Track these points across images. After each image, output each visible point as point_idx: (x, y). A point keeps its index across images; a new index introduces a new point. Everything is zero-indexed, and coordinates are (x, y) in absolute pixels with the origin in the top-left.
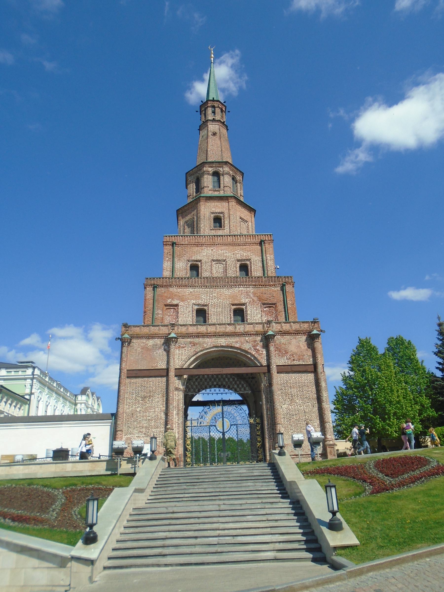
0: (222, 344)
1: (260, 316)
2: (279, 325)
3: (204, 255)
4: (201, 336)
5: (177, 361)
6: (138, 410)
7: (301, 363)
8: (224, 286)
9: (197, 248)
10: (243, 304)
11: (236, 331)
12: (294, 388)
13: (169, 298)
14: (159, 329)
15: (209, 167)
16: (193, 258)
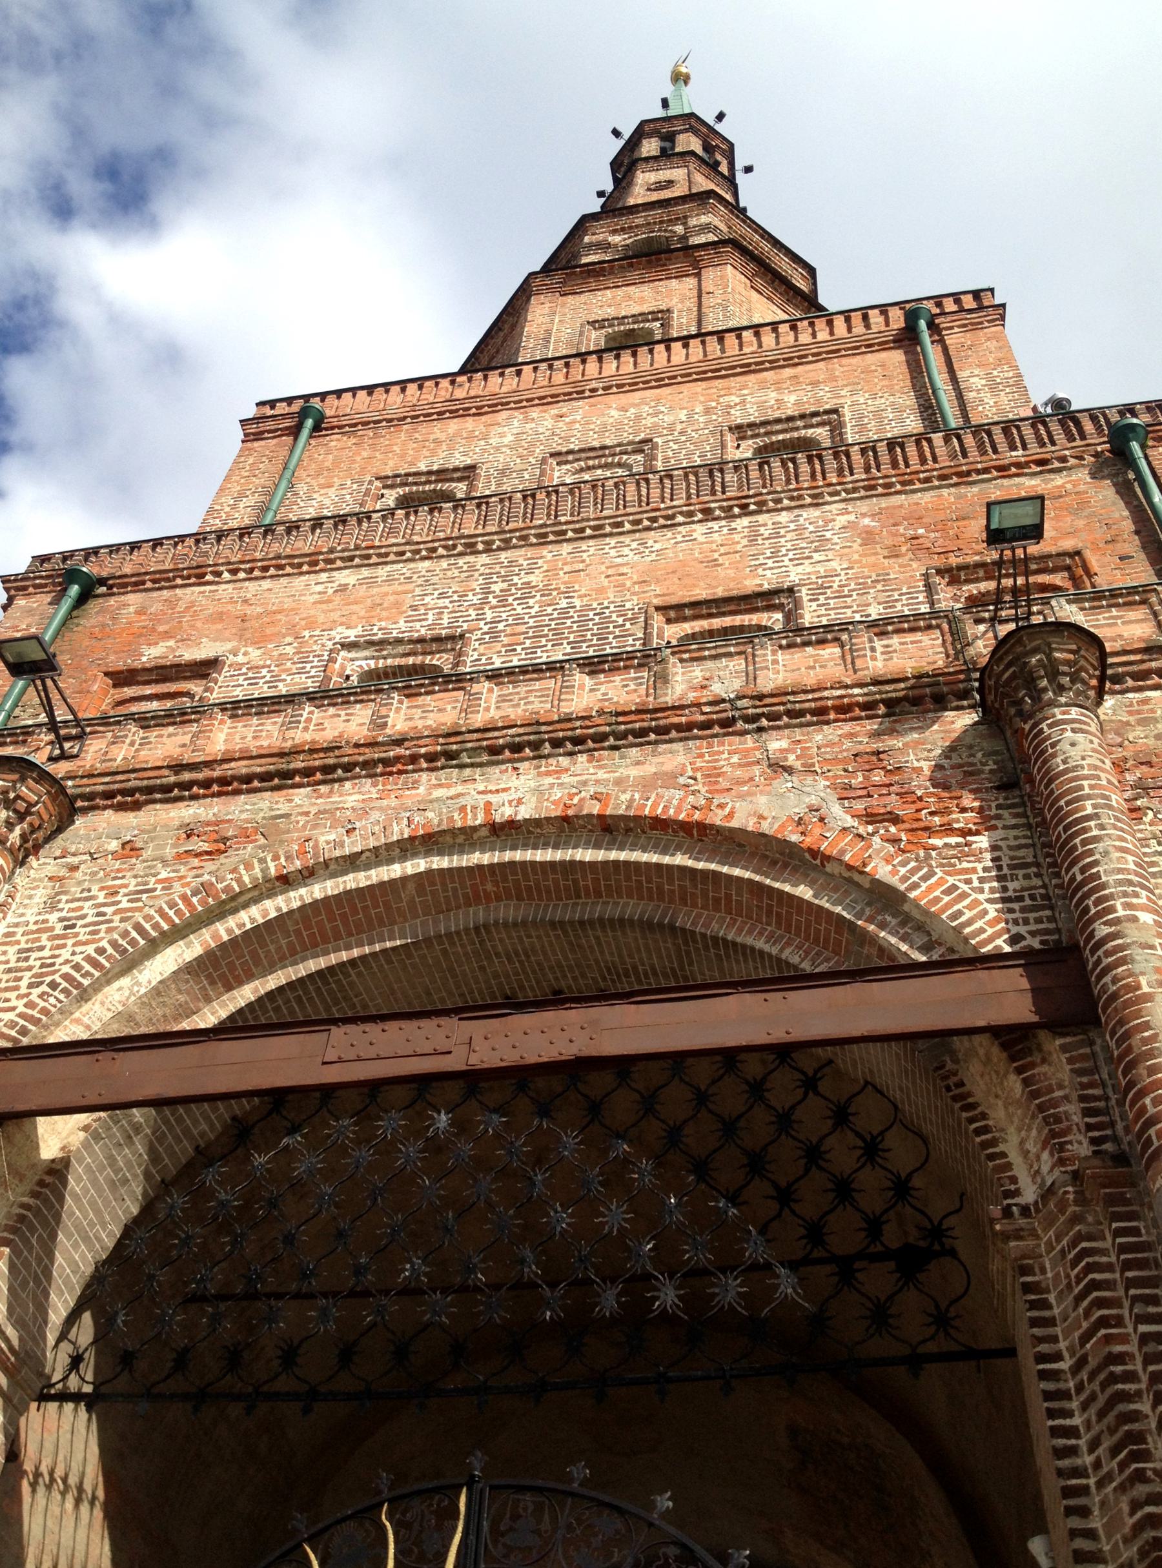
0: (504, 813)
2: (1133, 615)
4: (308, 772)
9: (453, 425)
11: (669, 699)
13: (167, 635)
15: (615, 232)
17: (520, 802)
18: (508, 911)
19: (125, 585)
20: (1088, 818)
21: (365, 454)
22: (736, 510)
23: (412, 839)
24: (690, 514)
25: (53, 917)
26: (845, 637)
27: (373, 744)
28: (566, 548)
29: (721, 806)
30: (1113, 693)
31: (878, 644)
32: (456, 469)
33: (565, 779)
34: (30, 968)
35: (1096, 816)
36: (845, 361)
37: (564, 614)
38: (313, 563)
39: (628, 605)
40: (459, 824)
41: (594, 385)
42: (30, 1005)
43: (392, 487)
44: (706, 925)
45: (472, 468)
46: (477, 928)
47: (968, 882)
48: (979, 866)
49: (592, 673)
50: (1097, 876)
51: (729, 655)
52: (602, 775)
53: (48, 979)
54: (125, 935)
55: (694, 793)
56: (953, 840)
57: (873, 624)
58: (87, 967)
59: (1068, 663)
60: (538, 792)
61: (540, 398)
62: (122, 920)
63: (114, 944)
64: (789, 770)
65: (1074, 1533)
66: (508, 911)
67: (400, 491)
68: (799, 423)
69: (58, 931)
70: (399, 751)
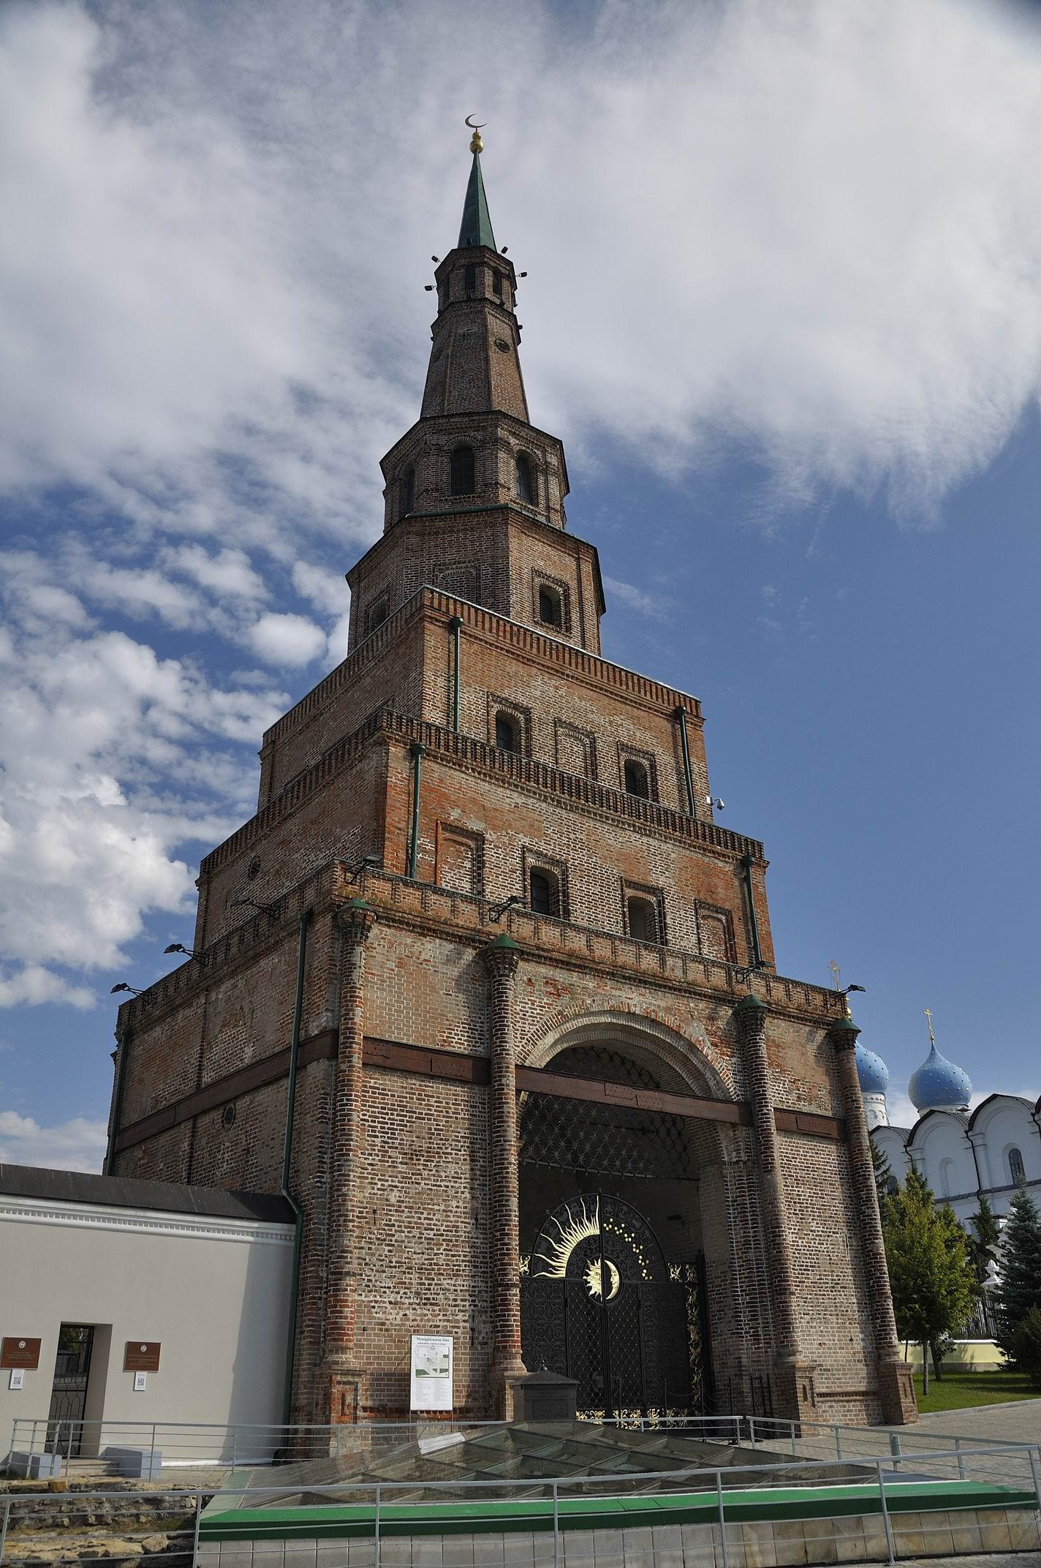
0: (633, 1009)
1: (694, 939)
3: (539, 693)
6: (393, 1200)
8: (603, 819)
13: (455, 805)
14: (454, 910)
18: (620, 1036)
28: (592, 823)
66: (620, 1036)
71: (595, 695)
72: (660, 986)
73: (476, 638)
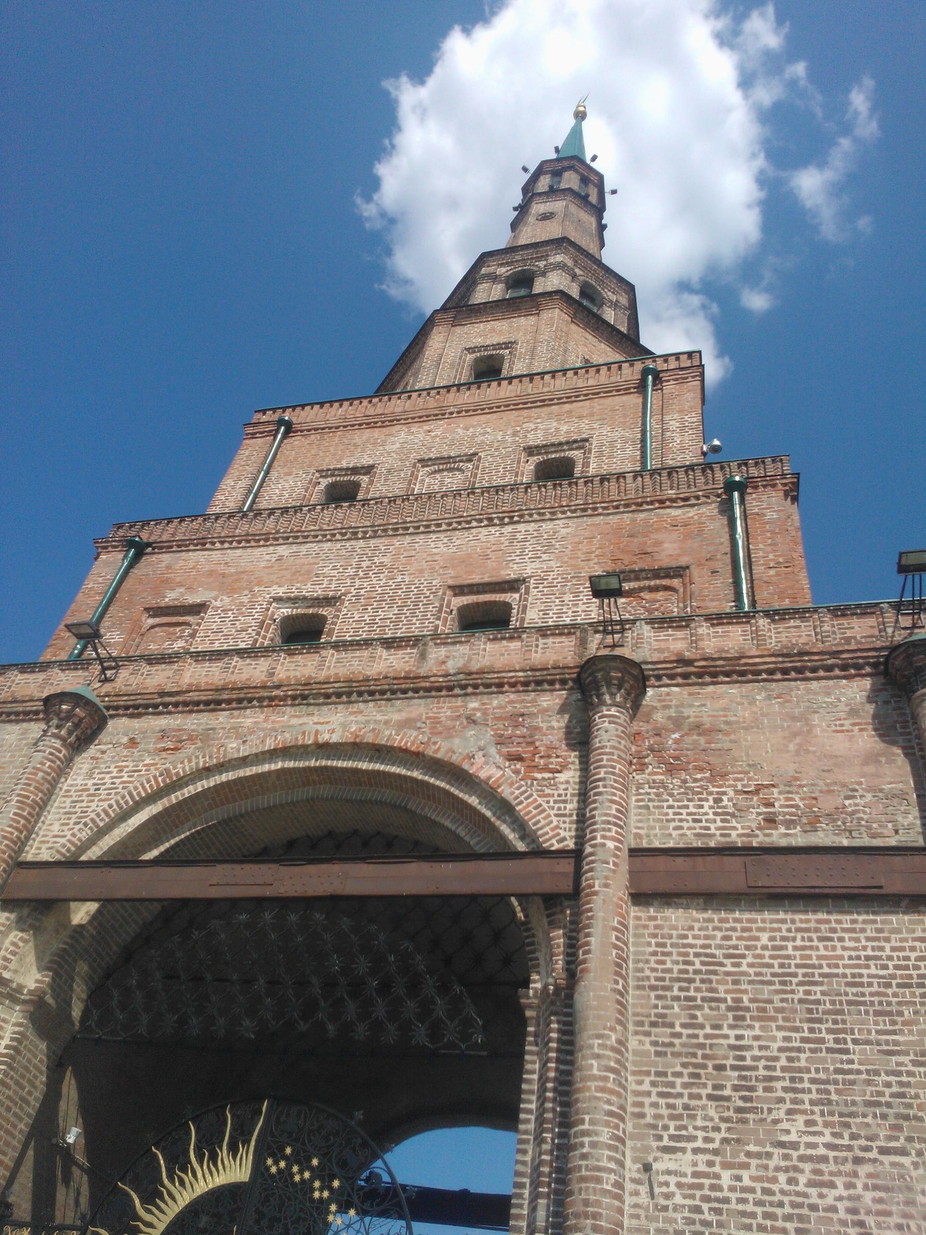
0: (324, 737)
2: (680, 634)
4: (229, 702)
5: (56, 827)
7: (822, 838)
9: (367, 433)
10: (512, 585)
11: (422, 672)
12: (763, 1017)
13: (181, 585)
16: (344, 464)
17: (333, 731)
19: (162, 548)
20: (599, 780)
21: (313, 452)
22: (507, 520)
23: (275, 750)
24: (480, 521)
25: (90, 782)
26: (524, 636)
27: (264, 687)
28: (408, 539)
29: (435, 743)
30: (654, 686)
31: (541, 641)
32: (363, 467)
33: (360, 718)
34: (75, 813)
35: (603, 779)
36: (602, 401)
37: (398, 585)
38: (266, 539)
39: (434, 583)
40: (300, 743)
41: (452, 409)
42: (74, 835)
43: (326, 477)
44: (423, 809)
45: (372, 467)
46: (307, 800)
47: (548, 802)
48: (556, 793)
49: (388, 648)
50: (593, 817)
51: (461, 642)
52: (379, 717)
53: (83, 820)
54: (123, 797)
55: (423, 733)
56: (547, 775)
57: (539, 629)
58: (103, 815)
59: (617, 678)
60: (344, 726)
61: (420, 417)
62: (124, 788)
63: (117, 802)
64: (474, 722)
65: (517, 1162)
66: (325, 791)
67: (330, 480)
68: (565, 447)
69: (92, 792)
70: (275, 693)
71: (494, 416)
72: (405, 692)
73: (316, 429)
